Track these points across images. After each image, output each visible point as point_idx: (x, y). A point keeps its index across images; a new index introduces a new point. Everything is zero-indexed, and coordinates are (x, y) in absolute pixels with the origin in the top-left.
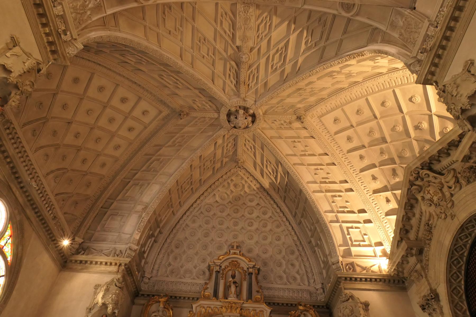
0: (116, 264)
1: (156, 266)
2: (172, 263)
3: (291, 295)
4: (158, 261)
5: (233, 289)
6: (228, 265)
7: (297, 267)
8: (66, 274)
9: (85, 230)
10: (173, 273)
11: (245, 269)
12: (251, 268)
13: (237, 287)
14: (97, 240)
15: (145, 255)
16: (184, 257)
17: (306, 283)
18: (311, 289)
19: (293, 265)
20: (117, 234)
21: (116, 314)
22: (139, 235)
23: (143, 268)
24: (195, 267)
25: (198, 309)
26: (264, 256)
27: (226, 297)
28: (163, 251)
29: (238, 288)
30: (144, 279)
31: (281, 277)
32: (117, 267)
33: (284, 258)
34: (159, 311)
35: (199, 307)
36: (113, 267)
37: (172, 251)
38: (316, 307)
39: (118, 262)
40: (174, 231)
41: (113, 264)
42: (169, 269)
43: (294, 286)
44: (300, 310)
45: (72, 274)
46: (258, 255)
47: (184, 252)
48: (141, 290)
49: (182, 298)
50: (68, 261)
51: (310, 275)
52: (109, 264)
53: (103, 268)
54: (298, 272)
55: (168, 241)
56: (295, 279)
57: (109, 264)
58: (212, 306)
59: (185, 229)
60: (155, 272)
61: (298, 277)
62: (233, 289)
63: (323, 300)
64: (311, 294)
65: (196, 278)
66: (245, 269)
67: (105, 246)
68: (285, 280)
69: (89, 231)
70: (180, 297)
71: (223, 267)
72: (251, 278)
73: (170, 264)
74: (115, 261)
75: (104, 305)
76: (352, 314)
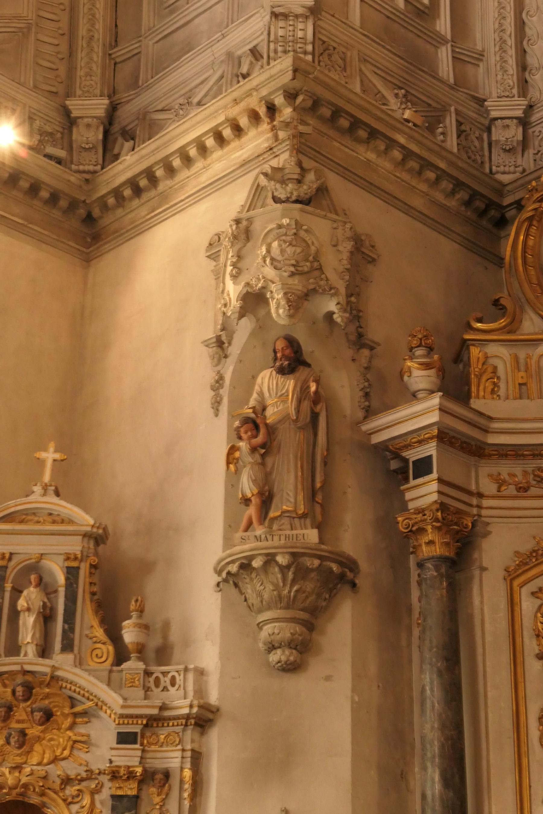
0: (255, 117)
8: (108, 262)
9: (98, 56)
15: (443, 25)
21: (337, 317)
23: (460, 82)
30: (498, 134)
32: (265, 126)
36: (252, 133)
39: (254, 102)
41: (244, 122)
45: (125, 250)
48: (500, 189)
50: (96, 212)
52: (227, 132)
53: (221, 162)
57: (227, 132)
67: (195, 68)
69: (120, 52)
74: (243, 105)
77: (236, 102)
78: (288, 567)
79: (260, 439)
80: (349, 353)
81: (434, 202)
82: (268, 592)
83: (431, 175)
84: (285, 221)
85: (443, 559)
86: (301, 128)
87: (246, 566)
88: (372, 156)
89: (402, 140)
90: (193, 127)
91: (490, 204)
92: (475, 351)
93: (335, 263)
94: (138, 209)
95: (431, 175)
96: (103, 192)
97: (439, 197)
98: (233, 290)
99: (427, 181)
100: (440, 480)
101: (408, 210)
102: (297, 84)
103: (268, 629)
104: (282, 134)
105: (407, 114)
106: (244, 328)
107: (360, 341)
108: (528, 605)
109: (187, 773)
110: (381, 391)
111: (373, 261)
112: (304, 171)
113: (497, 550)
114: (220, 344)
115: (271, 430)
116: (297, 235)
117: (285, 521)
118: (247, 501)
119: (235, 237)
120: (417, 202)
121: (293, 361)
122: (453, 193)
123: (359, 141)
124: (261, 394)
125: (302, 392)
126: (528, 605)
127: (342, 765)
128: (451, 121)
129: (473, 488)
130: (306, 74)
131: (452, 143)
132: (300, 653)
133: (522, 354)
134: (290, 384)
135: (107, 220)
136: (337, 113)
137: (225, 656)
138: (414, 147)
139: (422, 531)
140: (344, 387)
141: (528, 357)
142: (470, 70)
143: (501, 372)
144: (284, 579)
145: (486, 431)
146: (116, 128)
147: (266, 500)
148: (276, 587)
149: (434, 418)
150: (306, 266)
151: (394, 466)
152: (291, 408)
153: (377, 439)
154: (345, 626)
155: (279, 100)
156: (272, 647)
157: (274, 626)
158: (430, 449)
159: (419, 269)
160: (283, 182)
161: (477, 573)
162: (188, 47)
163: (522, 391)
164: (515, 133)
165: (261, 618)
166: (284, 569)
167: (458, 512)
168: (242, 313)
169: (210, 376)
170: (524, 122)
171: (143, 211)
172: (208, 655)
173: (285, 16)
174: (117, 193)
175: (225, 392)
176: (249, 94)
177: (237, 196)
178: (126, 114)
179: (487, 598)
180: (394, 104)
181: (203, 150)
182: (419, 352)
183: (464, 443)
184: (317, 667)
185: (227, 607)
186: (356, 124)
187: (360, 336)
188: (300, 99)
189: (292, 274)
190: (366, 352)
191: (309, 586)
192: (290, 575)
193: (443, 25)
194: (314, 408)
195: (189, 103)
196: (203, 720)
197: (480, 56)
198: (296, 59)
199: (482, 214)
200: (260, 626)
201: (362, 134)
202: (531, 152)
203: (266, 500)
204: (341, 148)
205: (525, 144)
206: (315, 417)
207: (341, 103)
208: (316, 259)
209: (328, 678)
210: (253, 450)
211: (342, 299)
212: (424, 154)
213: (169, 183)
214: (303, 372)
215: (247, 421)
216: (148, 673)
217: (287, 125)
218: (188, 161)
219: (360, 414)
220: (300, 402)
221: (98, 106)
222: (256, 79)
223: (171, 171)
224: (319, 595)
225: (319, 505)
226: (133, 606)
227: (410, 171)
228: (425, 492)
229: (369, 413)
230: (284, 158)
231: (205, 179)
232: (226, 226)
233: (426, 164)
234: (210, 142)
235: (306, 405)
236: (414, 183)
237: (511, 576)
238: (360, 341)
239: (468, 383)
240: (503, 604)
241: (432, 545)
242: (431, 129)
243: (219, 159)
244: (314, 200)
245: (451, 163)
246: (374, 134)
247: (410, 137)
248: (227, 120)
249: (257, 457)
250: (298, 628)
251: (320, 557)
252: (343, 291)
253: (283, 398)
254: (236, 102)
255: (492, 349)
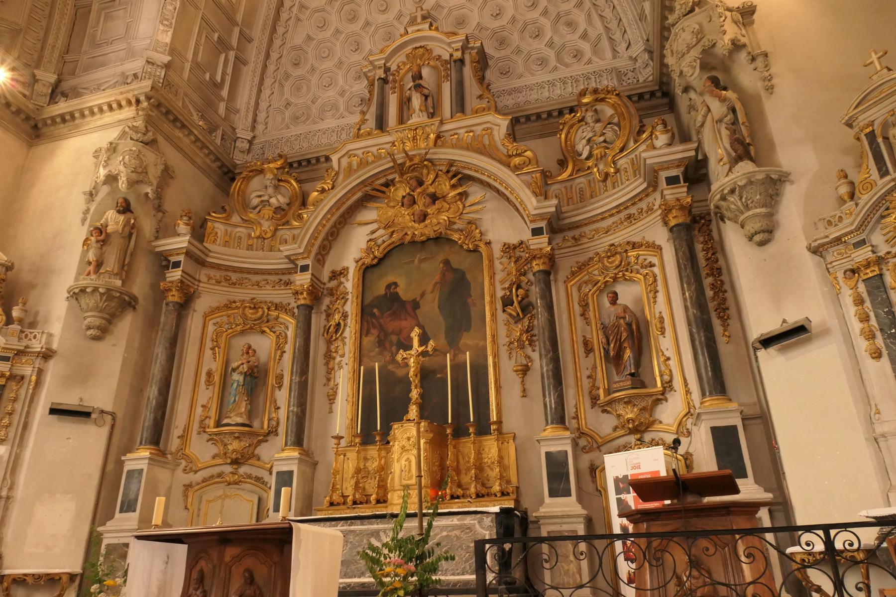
0: (129, 103)
1: (261, 116)
2: (293, 100)
3: (570, 89)
4: (263, 105)
5: (417, 101)
6: (405, 60)
7: (582, 26)
8: (41, 149)
10: (297, 118)
11: (447, 57)
12: (457, 50)
13: (426, 97)
14: (88, 69)
15: (225, 93)
16: (314, 79)
17: (608, 54)
18: (622, 63)
19: (569, 24)
20: (124, 46)
21: (150, 195)
22: (170, 33)
23: (226, 119)
24: (342, 93)
25: (345, 162)
26: (495, 24)
27: (401, 121)
28: (268, 82)
29: (430, 100)
30: (238, 144)
31: (543, 62)
32: (133, 108)
33: (545, 13)
34: (266, 187)
35: (346, 158)
36: (127, 109)
37: (287, 76)
38: (635, 98)
39: (130, 96)
40: (280, 30)
41: (124, 103)
42: (288, 114)
43: (578, 69)
44: (587, 104)
46: (480, 27)
47: (313, 69)
48: (235, 166)
49: (323, 159)
50: (40, 125)
51: (617, 36)
52: (114, 106)
53: (109, 118)
54: (584, 36)
55: (274, 56)
56: (578, 55)
57: (114, 106)
58: (374, 149)
59: (301, 16)
60: (260, 127)
61: (586, 47)
62: (417, 101)
63: (651, 78)
64: (620, 74)
65: (346, 114)
66: (447, 57)
68: (553, 62)
69: (68, 58)
70: (318, 159)
71: (394, 68)
72: (460, 72)
73: (288, 104)
75: (111, 179)
76: (698, 42)
77: (121, 93)
78: (104, 294)
79: (102, 238)
80: (154, 212)
81: (205, 163)
82: (92, 303)
83: (207, 151)
84: (134, 149)
85: (177, 303)
86: (150, 113)
87: (83, 290)
88: (181, 135)
89: (196, 132)
90: (98, 99)
91: (230, 171)
92: (209, 224)
93: (154, 173)
94: (63, 129)
95: (207, 151)
96: (46, 116)
97: (208, 162)
98: (102, 172)
99: (204, 153)
100: (183, 271)
101: (193, 162)
102: (152, 94)
103: (89, 320)
104: (140, 113)
105: (201, 123)
106: (105, 190)
107: (159, 208)
108: (211, 328)
109: (34, 378)
110: (164, 230)
111: (172, 178)
112: (147, 131)
113: (202, 304)
114: (91, 195)
115: (108, 235)
116: (138, 156)
117: (107, 275)
118: (90, 263)
119: (108, 149)
120: (198, 161)
121: (125, 208)
122: (214, 161)
123: (176, 127)
124: (107, 219)
125: (127, 222)
126: (211, 328)
127: (114, 382)
128: (219, 133)
129: (197, 277)
130: (157, 91)
131: (218, 141)
132: (102, 332)
133: (229, 229)
134: (122, 218)
135: (45, 130)
136: (168, 112)
137: (64, 329)
138: (201, 137)
139: (170, 290)
140: (148, 225)
141: (231, 232)
142: (232, 115)
143: (219, 235)
144: (101, 299)
145: (207, 256)
146: (59, 90)
147: (99, 264)
148: (96, 302)
149: (185, 245)
150: (140, 170)
151: (164, 262)
152: (120, 228)
153: (158, 249)
154: (127, 326)
155: (142, 98)
156: (89, 328)
157: (93, 319)
158: (181, 258)
159: (191, 187)
160: (137, 132)
161: (191, 312)
162: (103, 65)
163: (226, 244)
164: (246, 146)
165: (86, 314)
166: (102, 295)
167: (188, 285)
168: (105, 183)
169: (84, 207)
170: (250, 142)
171: (65, 131)
172: (56, 328)
173: (153, 64)
174: (53, 119)
175: (89, 216)
176: (128, 92)
177: (113, 134)
178: (66, 86)
179: (194, 323)
180: (195, 117)
181: (101, 110)
182: (185, 218)
183: (197, 259)
184: (109, 340)
185: (69, 309)
186: (176, 119)
187: (159, 206)
188: (152, 100)
189: (132, 172)
190: (161, 214)
191: (113, 304)
192: (104, 298)
193: (225, 93)
194: (131, 231)
195: (98, 88)
196: (47, 355)
197: (238, 111)
198: (154, 82)
199: (225, 174)
200: (85, 318)
201: (178, 124)
202: (251, 155)
203: (99, 264)
204: (167, 127)
205: (249, 151)
206: (131, 235)
207: (171, 108)
208: (145, 168)
209: (114, 345)
210: (98, 241)
211: (154, 187)
212: (205, 141)
213: (81, 121)
214: (129, 215)
215: (96, 228)
216: (22, 332)
217: (144, 109)
218: (93, 113)
219: (153, 239)
220: (125, 226)
221: (52, 78)
222: (132, 87)
223: (83, 116)
224: (117, 309)
225: (125, 270)
226: (20, 301)
227: (197, 146)
228: (175, 275)
229: (157, 238)
230: (139, 123)
231: (99, 123)
232: (104, 145)
233: (204, 146)
234: (105, 108)
235: (127, 229)
236: (198, 152)
237: (206, 316)
238: (159, 208)
239: (204, 236)
240: (200, 326)
241: (174, 297)
242: (210, 133)
243: (108, 116)
244: (151, 144)
245: (215, 149)
246: (183, 126)
247: (200, 133)
248: (115, 100)
249: (99, 245)
250: (104, 321)
251: (121, 293)
252: (155, 183)
253: (117, 223)
254: (121, 93)
255: (217, 225)
